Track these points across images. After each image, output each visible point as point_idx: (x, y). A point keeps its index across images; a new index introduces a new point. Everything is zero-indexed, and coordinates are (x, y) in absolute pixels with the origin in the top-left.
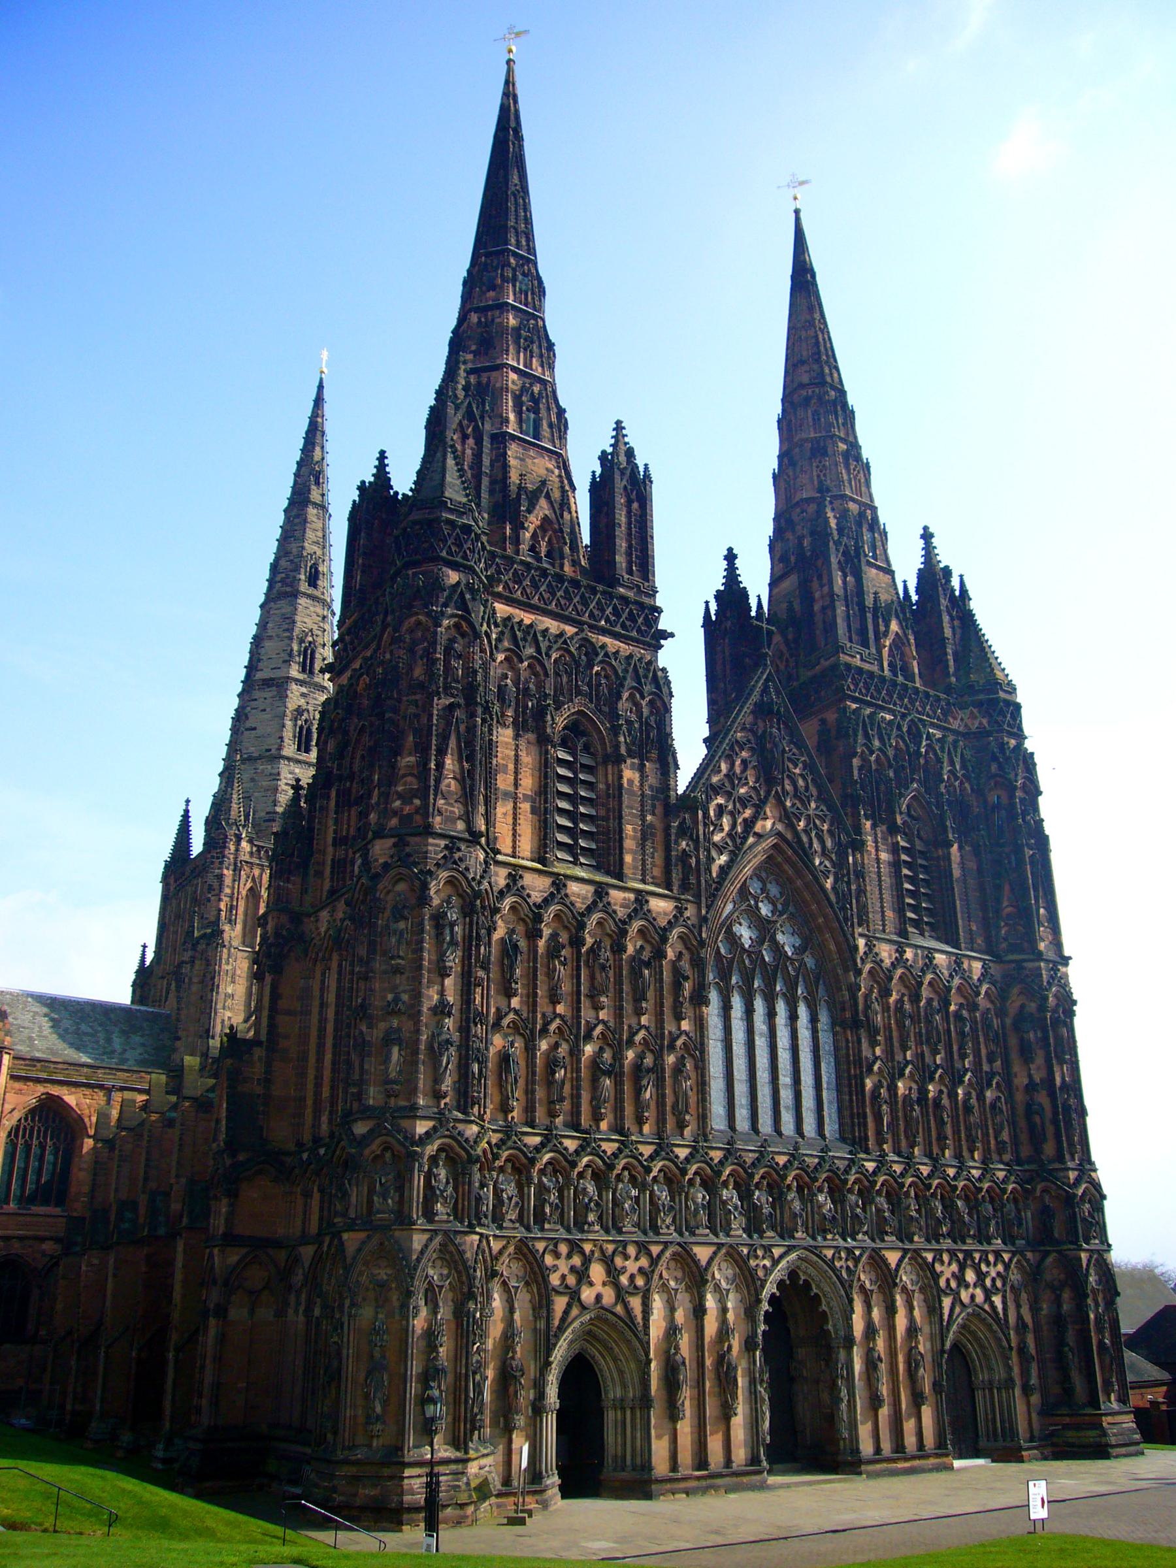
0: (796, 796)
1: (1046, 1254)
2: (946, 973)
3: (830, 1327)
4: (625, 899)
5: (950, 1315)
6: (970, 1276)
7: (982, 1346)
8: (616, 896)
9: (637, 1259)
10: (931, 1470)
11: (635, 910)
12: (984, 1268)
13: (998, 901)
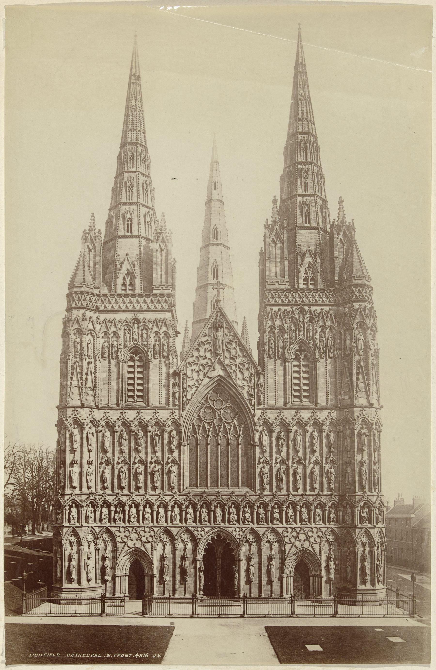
6: (302, 537)
7: (312, 562)
12: (310, 534)
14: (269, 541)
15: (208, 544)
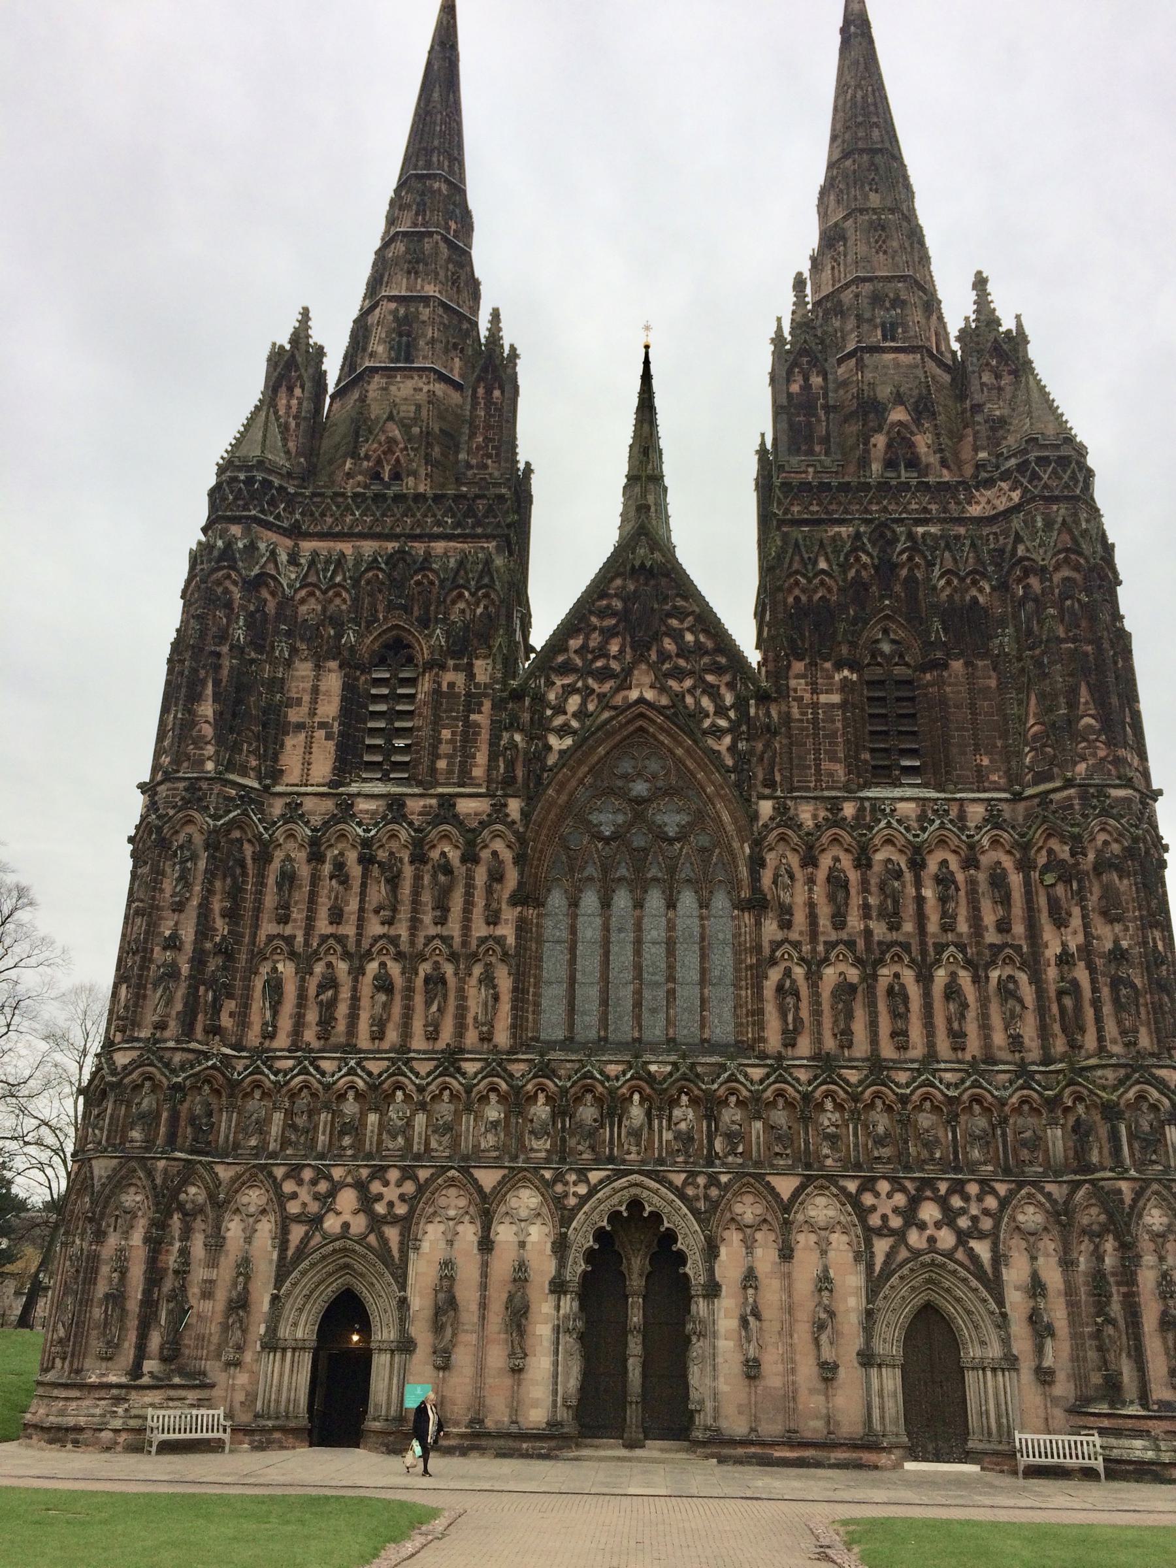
0: (678, 655)
1: (1076, 1185)
2: (915, 825)
3: (689, 1270)
4: (425, 806)
5: (886, 1263)
6: (929, 1212)
7: (969, 1313)
8: (414, 806)
9: (399, 1184)
10: (832, 1466)
11: (437, 815)
12: (956, 1202)
13: (1022, 720)
14: (810, 1224)
15: (600, 1234)
